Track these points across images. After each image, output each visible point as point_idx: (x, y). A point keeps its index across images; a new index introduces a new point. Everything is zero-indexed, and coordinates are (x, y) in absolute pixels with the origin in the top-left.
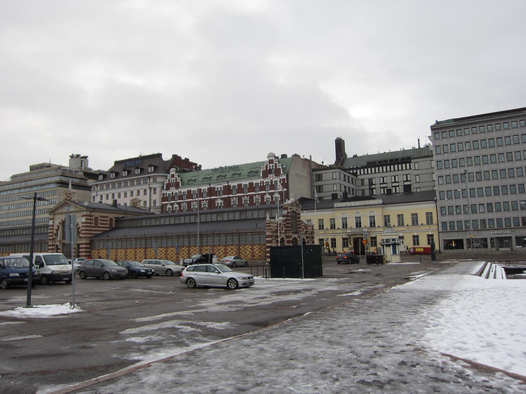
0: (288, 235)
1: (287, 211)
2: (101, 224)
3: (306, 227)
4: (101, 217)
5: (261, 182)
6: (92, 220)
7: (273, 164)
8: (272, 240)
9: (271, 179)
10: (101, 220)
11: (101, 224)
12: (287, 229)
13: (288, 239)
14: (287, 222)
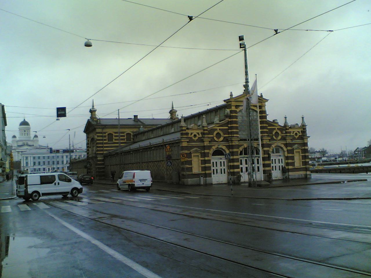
0: (230, 144)
1: (231, 109)
2: (115, 140)
3: (285, 128)
4: (115, 133)
6: (105, 136)
8: (191, 153)
10: (115, 136)
11: (115, 140)
12: (230, 135)
13: (231, 150)
14: (229, 126)
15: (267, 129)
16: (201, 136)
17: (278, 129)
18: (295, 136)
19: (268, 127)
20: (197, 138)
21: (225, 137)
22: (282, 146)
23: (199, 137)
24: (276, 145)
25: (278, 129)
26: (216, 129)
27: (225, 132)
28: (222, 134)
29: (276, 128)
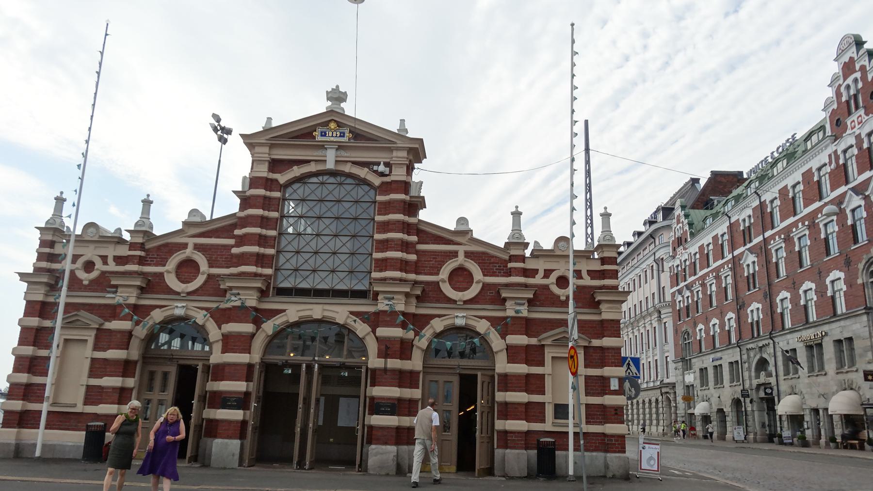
5: (830, 156)
7: (856, 71)
9: (857, 133)
14: (237, 232)
15: (417, 252)
16: (112, 267)
17: (466, 257)
18: (555, 289)
19: (421, 247)
20: (94, 274)
21: (210, 277)
22: (482, 326)
23: (103, 273)
24: (447, 322)
25: (468, 255)
26: (185, 246)
27: (215, 255)
28: (202, 261)
29: (461, 250)
